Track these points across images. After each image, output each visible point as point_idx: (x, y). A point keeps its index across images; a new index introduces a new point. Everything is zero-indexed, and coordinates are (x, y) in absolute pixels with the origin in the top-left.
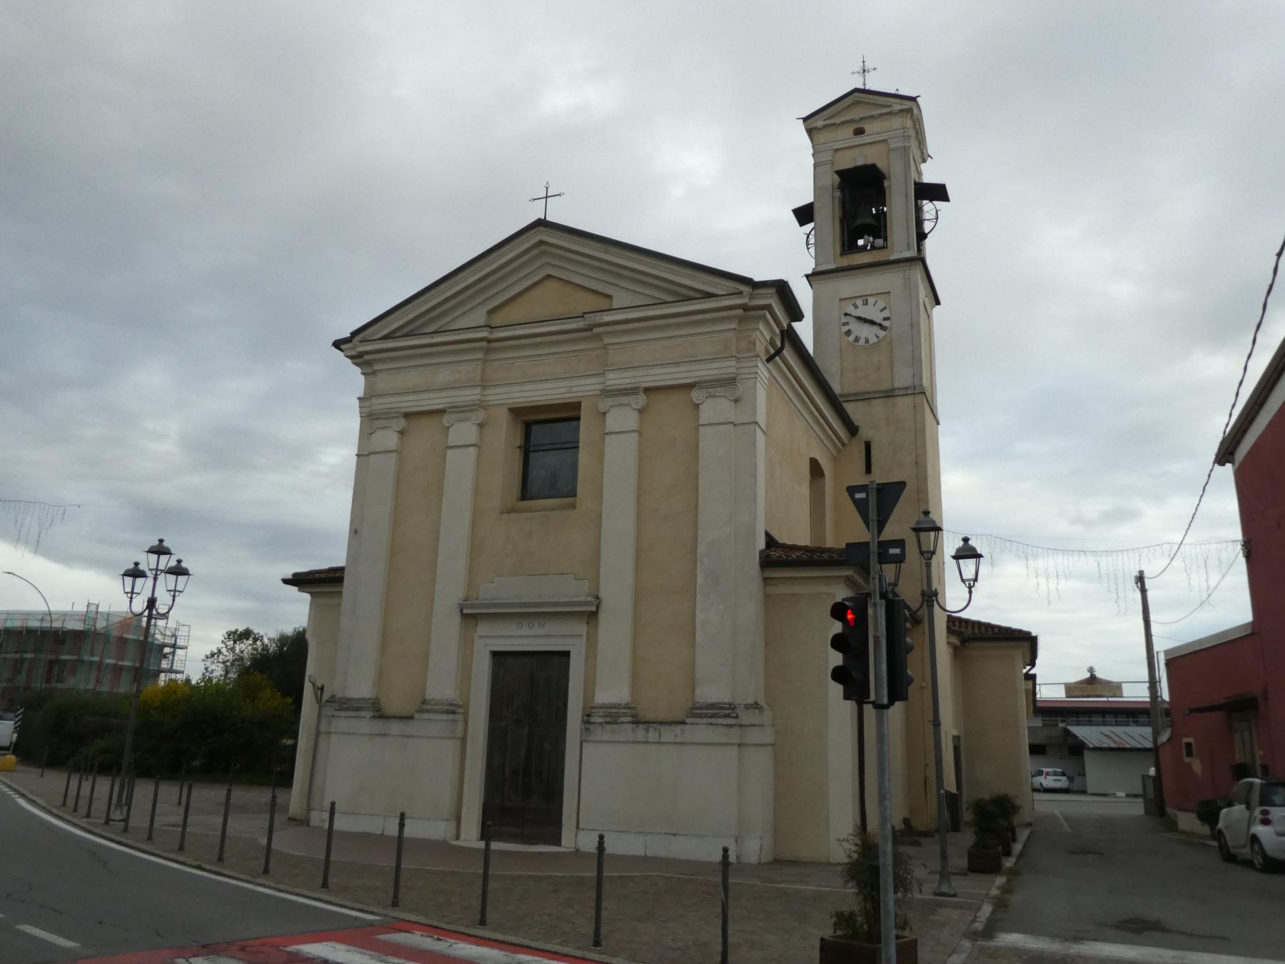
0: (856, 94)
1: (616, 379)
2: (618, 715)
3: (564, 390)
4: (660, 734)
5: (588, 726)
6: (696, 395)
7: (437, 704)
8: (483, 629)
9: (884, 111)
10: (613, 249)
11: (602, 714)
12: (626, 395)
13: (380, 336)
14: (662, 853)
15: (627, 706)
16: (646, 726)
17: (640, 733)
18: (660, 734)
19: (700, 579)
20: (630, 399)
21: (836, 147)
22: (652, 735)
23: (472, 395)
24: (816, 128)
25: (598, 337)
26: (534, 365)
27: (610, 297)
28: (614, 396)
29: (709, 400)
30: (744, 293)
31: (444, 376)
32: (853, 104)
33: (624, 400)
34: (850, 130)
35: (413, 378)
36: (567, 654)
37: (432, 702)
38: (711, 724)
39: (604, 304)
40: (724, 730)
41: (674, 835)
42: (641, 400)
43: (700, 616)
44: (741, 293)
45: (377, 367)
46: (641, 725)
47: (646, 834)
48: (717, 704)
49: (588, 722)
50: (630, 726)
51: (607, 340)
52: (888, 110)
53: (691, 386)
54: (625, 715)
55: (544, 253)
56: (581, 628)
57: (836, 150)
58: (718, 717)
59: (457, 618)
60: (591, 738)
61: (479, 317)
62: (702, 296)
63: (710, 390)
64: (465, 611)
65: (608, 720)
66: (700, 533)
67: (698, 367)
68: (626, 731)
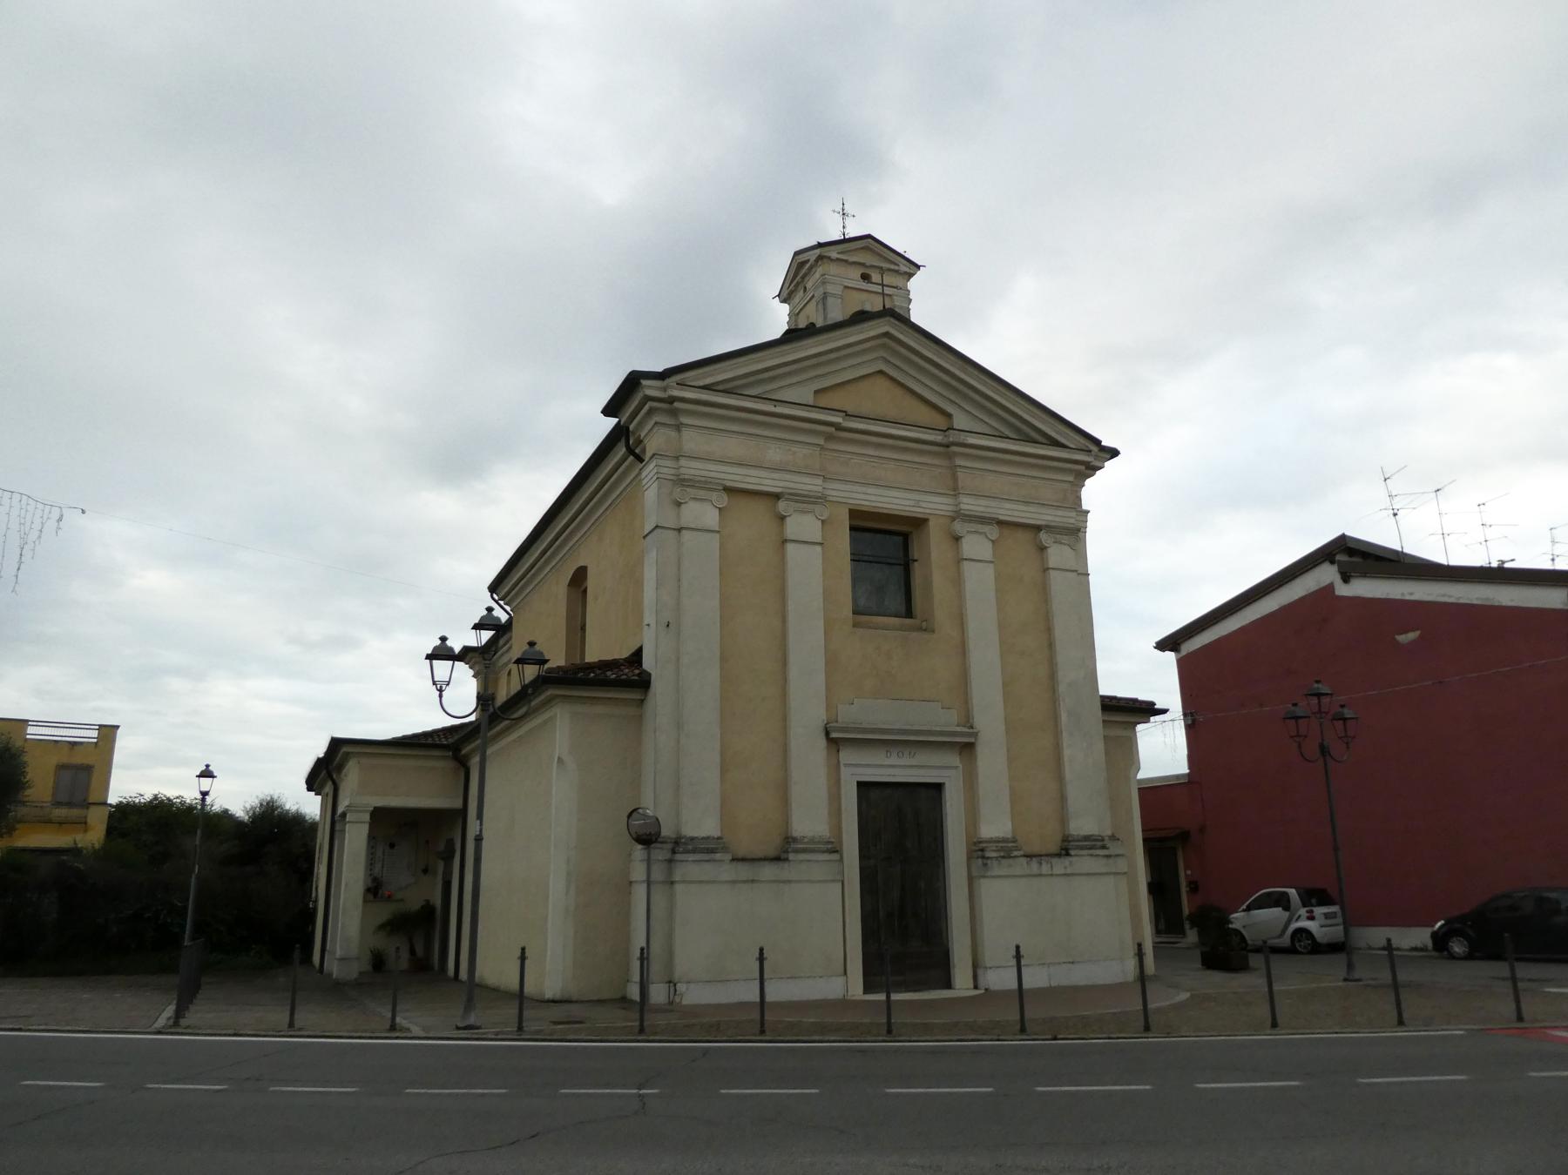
0: (870, 240)
1: (969, 504)
2: (1011, 850)
3: (912, 503)
4: (1052, 867)
5: (985, 861)
6: (1044, 537)
7: (812, 841)
8: (846, 756)
9: (892, 267)
10: (970, 369)
11: (994, 848)
12: (982, 523)
13: (701, 383)
14: (1065, 982)
15: (1014, 841)
16: (1039, 859)
17: (1034, 867)
18: (1052, 867)
19: (1064, 717)
20: (986, 529)
21: (846, 284)
22: (1045, 869)
23: (811, 485)
24: (829, 258)
25: (950, 457)
26: (874, 466)
27: (949, 416)
28: (970, 521)
29: (1056, 545)
30: (1093, 452)
31: (774, 454)
32: (862, 248)
33: (980, 527)
34: (856, 273)
35: (733, 446)
36: (938, 788)
37: (806, 840)
38: (1091, 855)
39: (940, 422)
40: (1104, 861)
41: (1073, 963)
42: (993, 532)
43: (1067, 753)
44: (1090, 451)
45: (685, 420)
46: (1034, 859)
47: (1049, 964)
48: (1092, 836)
49: (983, 857)
50: (1023, 860)
51: (959, 462)
52: (896, 268)
53: (1038, 528)
54: (1017, 849)
55: (884, 346)
56: (953, 759)
57: (846, 287)
58: (1096, 849)
59: (822, 742)
60: (989, 874)
61: (805, 394)
62: (1045, 441)
63: (1058, 536)
64: (834, 735)
65: (1002, 854)
66: (1060, 674)
67: (1043, 510)
68: (1021, 866)
